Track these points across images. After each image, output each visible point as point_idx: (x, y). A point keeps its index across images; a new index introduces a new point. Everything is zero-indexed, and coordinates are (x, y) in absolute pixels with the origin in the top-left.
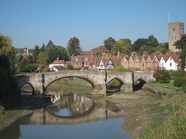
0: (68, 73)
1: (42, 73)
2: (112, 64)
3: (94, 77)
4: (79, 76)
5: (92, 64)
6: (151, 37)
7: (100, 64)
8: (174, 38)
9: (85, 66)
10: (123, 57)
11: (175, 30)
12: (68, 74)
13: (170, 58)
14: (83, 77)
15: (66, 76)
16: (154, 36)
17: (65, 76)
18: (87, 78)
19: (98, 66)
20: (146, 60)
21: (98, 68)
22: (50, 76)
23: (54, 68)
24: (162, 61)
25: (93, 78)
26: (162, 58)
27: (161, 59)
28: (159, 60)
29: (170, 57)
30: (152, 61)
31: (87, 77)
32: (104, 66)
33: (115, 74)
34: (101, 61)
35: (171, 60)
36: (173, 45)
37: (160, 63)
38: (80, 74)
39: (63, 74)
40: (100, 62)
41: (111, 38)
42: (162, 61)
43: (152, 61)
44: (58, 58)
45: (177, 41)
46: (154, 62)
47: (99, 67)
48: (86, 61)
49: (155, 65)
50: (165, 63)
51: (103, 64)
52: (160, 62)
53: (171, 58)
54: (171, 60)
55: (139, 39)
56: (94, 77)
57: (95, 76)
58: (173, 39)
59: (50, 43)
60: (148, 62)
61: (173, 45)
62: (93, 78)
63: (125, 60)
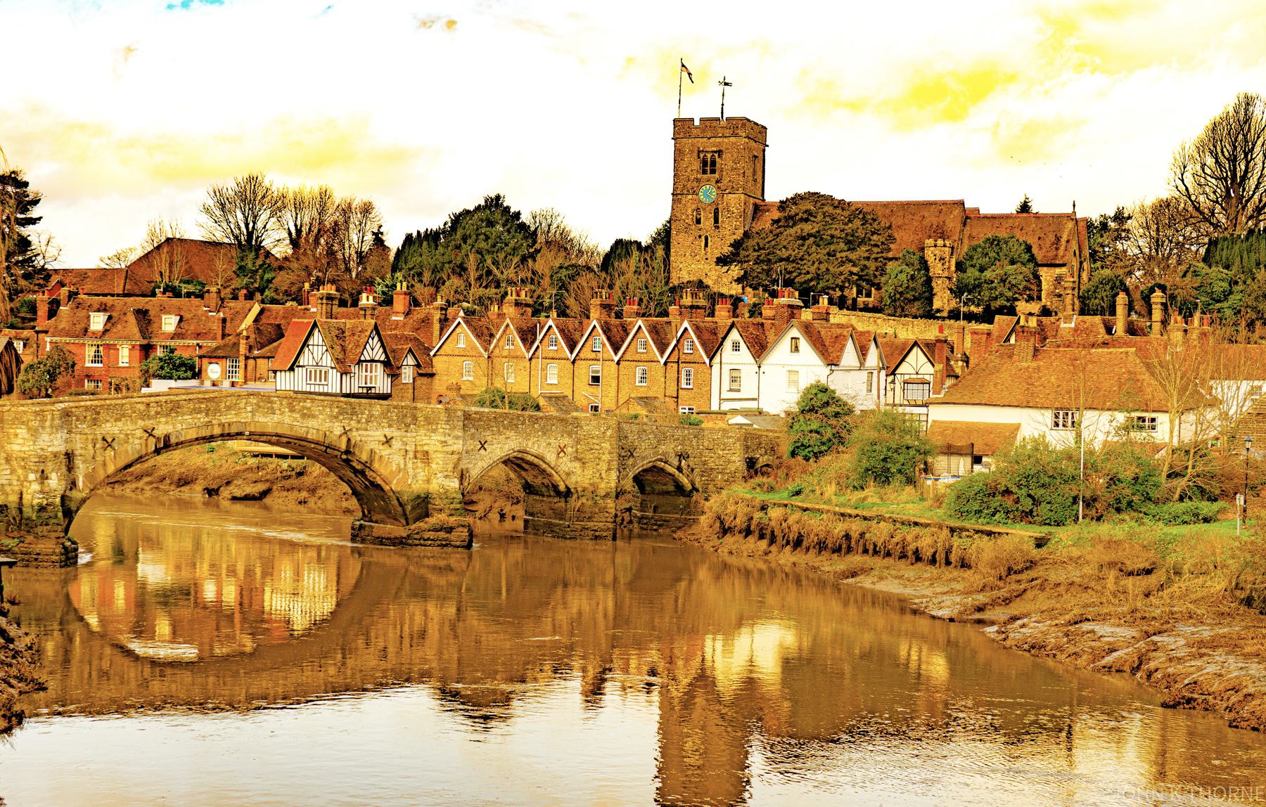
0: (229, 408)
2: (386, 364)
4: (301, 432)
7: (305, 359)
8: (707, 223)
10: (444, 322)
11: (713, 163)
13: (785, 343)
17: (205, 432)
19: (291, 369)
20: (616, 350)
21: (285, 382)
25: (385, 451)
26: (735, 335)
27: (728, 344)
28: (713, 346)
30: (662, 353)
31: (344, 439)
32: (334, 376)
33: (513, 426)
34: (317, 338)
38: (304, 416)
40: (305, 344)
42: (735, 355)
43: (662, 353)
51: (328, 361)
52: (717, 359)
56: (388, 441)
57: (396, 433)
58: (698, 221)
60: (627, 357)
63: (464, 337)
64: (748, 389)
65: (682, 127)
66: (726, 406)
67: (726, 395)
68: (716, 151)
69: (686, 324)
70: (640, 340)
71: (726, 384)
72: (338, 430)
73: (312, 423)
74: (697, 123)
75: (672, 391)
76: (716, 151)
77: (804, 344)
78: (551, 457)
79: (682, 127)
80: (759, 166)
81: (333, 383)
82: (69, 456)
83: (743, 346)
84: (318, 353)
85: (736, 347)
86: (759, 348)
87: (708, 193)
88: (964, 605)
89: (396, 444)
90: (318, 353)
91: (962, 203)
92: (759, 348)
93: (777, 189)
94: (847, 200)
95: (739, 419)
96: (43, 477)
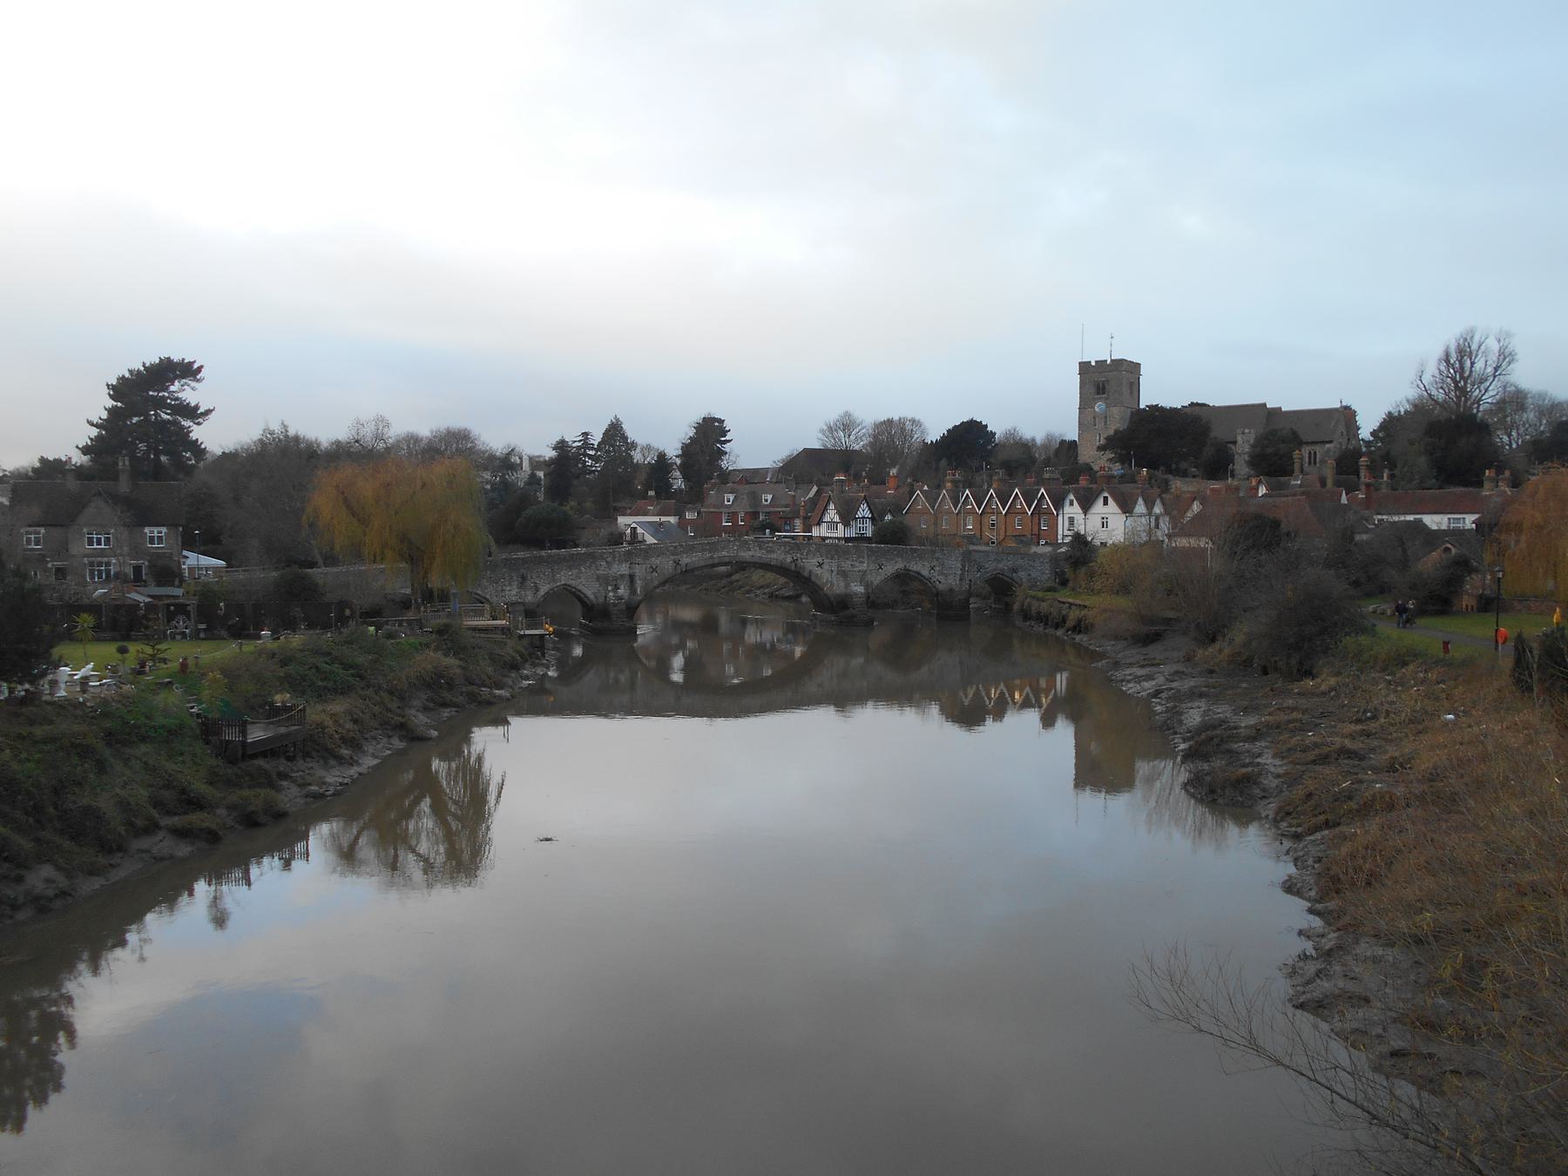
1: (1241, 466)
3: (820, 565)
8: (1100, 425)
19: (819, 524)
23: (639, 530)
24: (1072, 510)
28: (1059, 504)
34: (832, 506)
35: (1106, 503)
40: (825, 509)
42: (1072, 510)
44: (652, 493)
45: (1116, 432)
46: (1038, 511)
51: (837, 519)
53: (1106, 499)
54: (1106, 503)
56: (820, 565)
59: (615, 432)
61: (1100, 448)
62: (819, 571)
65: (1085, 368)
68: (1106, 380)
72: (789, 560)
73: (774, 556)
75: (1036, 531)
76: (1106, 380)
77: (1110, 500)
78: (925, 572)
79: (1085, 368)
81: (840, 531)
82: (632, 577)
84: (832, 514)
86: (1086, 506)
87: (1099, 407)
88: (534, 665)
89: (826, 567)
90: (832, 514)
92: (1086, 506)
94: (896, 418)
96: (616, 588)
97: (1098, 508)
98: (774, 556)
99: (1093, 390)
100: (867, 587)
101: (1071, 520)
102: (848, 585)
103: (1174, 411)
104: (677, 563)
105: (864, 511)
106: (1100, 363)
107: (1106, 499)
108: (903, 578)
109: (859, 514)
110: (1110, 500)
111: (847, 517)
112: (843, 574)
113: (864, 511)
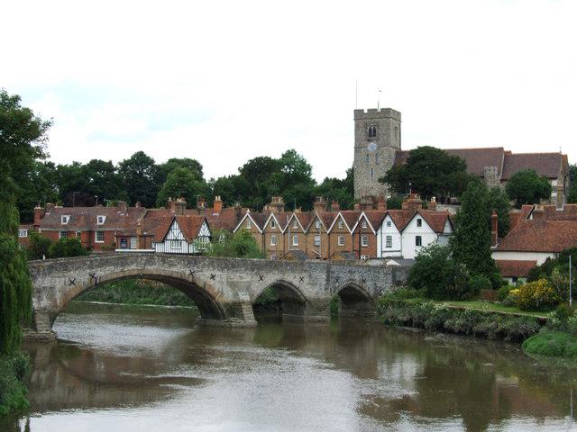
3: (213, 277)
4: (168, 274)
5: (126, 234)
6: (290, 156)
7: (170, 236)
8: (372, 161)
9: (96, 241)
11: (375, 131)
12: (133, 267)
13: (414, 222)
14: (179, 276)
15: (127, 274)
16: (299, 152)
18: (190, 280)
19: (163, 242)
21: (159, 248)
22: (73, 274)
24: (389, 229)
25: (212, 282)
26: (388, 219)
27: (385, 223)
28: (378, 225)
29: (418, 217)
34: (176, 226)
36: (380, 180)
37: (379, 236)
39: (116, 265)
40: (170, 229)
41: (141, 154)
42: (389, 229)
46: (359, 232)
47: (167, 247)
48: (100, 226)
49: (360, 242)
50: (399, 235)
51: (181, 237)
52: (379, 231)
53: (419, 221)
55: (261, 158)
56: (213, 277)
57: (217, 273)
62: (212, 282)
64: (396, 246)
65: (359, 114)
66: (385, 255)
67: (384, 249)
68: (375, 126)
69: (363, 214)
70: (340, 223)
71: (385, 244)
72: (188, 272)
74: (366, 111)
76: (375, 126)
77: (423, 222)
79: (359, 114)
80: (398, 132)
83: (392, 223)
84: (176, 232)
85: (389, 224)
87: (372, 146)
89: (217, 279)
90: (176, 232)
91: (502, 148)
93: (409, 143)
95: (392, 262)
97: (413, 229)
98: (175, 269)
99: (363, 136)
100: (251, 296)
101: (389, 239)
102: (236, 295)
103: (439, 150)
104: (92, 276)
105: (204, 231)
106: (372, 111)
107: (419, 221)
108: (279, 287)
109: (201, 234)
110: (423, 222)
111: (190, 236)
112: (233, 285)
113: (204, 231)
